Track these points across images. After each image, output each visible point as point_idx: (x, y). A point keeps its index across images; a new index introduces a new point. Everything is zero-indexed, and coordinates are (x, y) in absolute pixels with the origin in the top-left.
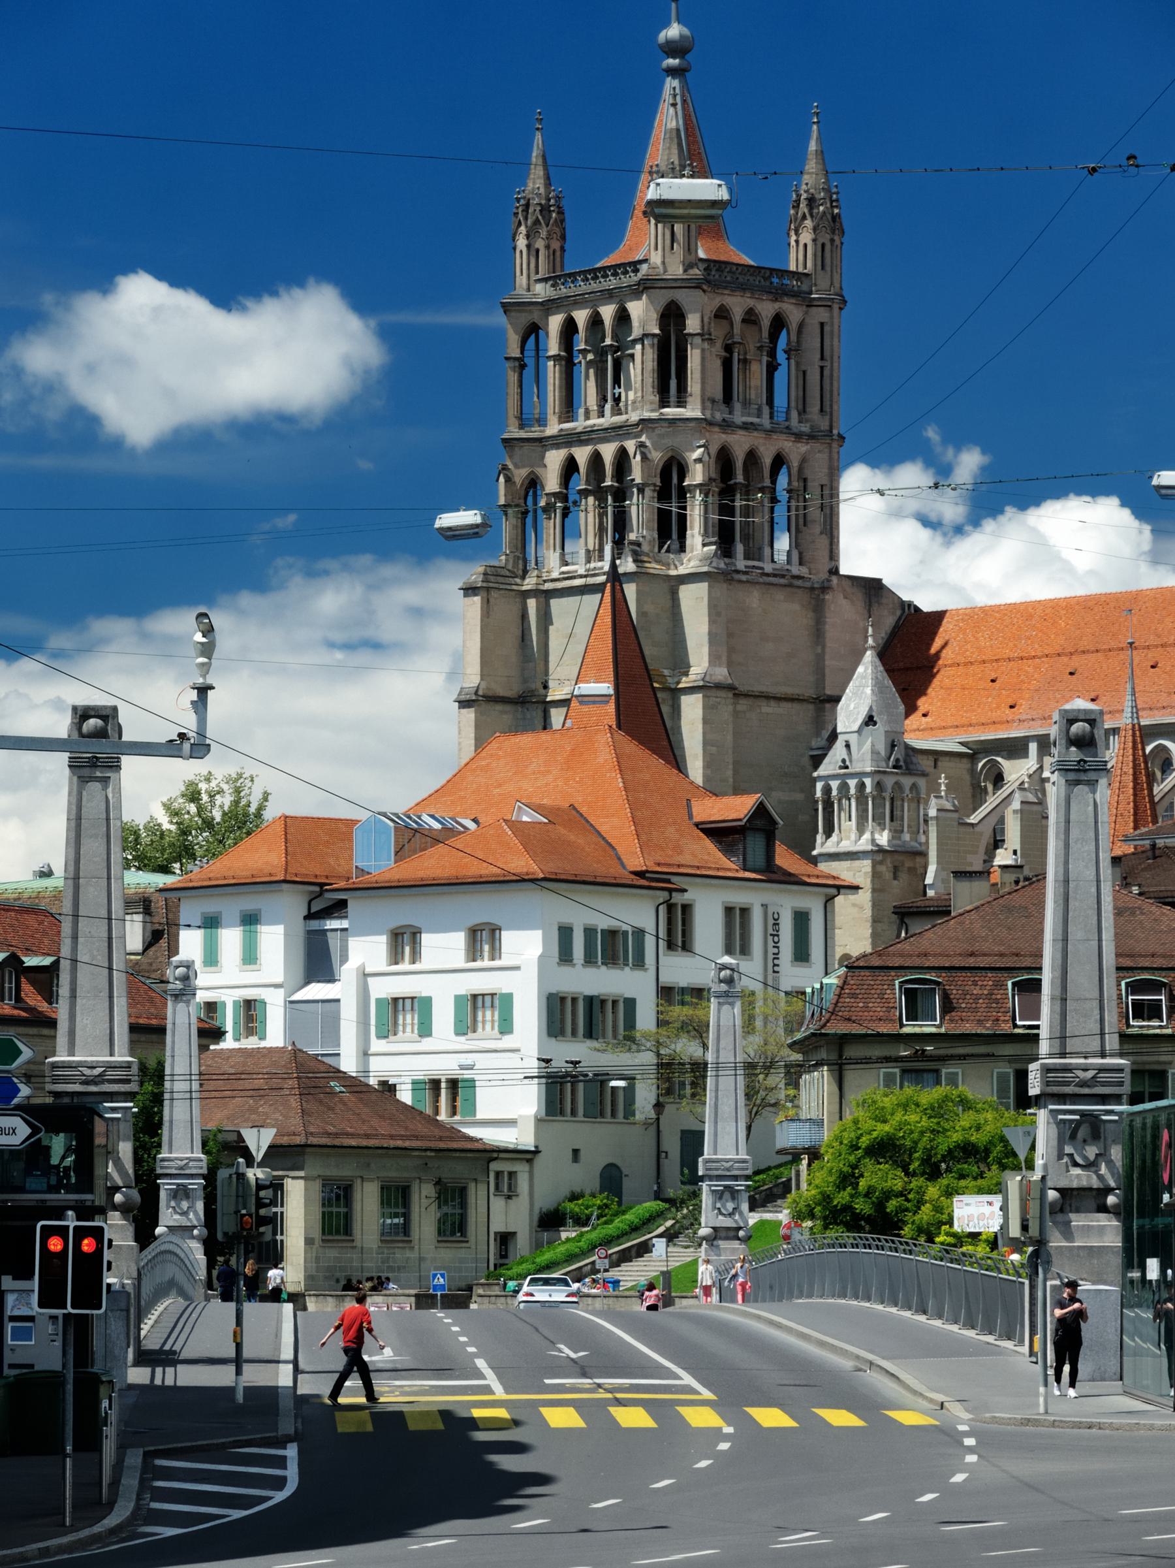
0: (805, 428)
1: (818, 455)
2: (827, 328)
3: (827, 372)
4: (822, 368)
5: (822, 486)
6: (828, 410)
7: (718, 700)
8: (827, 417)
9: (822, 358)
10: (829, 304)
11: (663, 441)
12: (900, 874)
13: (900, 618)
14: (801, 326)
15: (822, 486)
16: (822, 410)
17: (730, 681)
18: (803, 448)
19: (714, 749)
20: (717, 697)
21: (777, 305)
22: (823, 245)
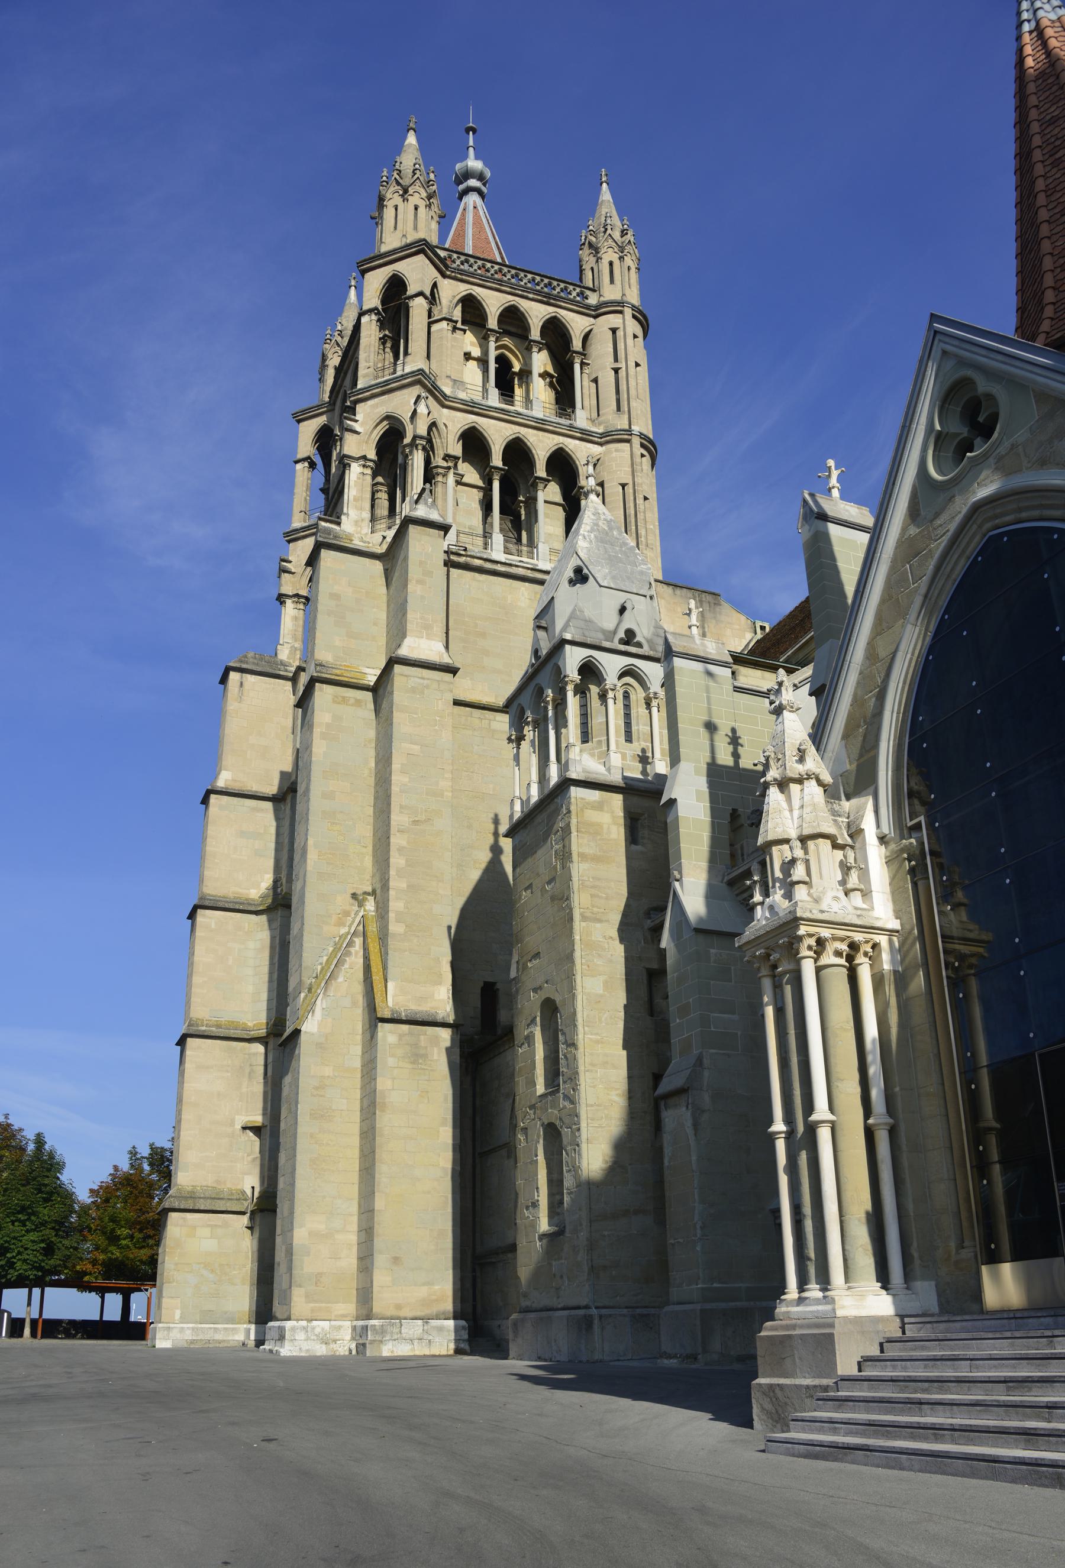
0: (600, 430)
1: (614, 454)
2: (620, 333)
3: (622, 374)
4: (616, 371)
5: (623, 486)
6: (626, 409)
7: (426, 682)
8: (626, 416)
9: (616, 360)
10: (620, 308)
11: (377, 410)
12: (643, 833)
13: (750, 641)
14: (586, 338)
15: (623, 486)
16: (619, 409)
17: (446, 660)
18: (596, 450)
19: (416, 748)
20: (423, 678)
21: (551, 309)
22: (611, 264)
